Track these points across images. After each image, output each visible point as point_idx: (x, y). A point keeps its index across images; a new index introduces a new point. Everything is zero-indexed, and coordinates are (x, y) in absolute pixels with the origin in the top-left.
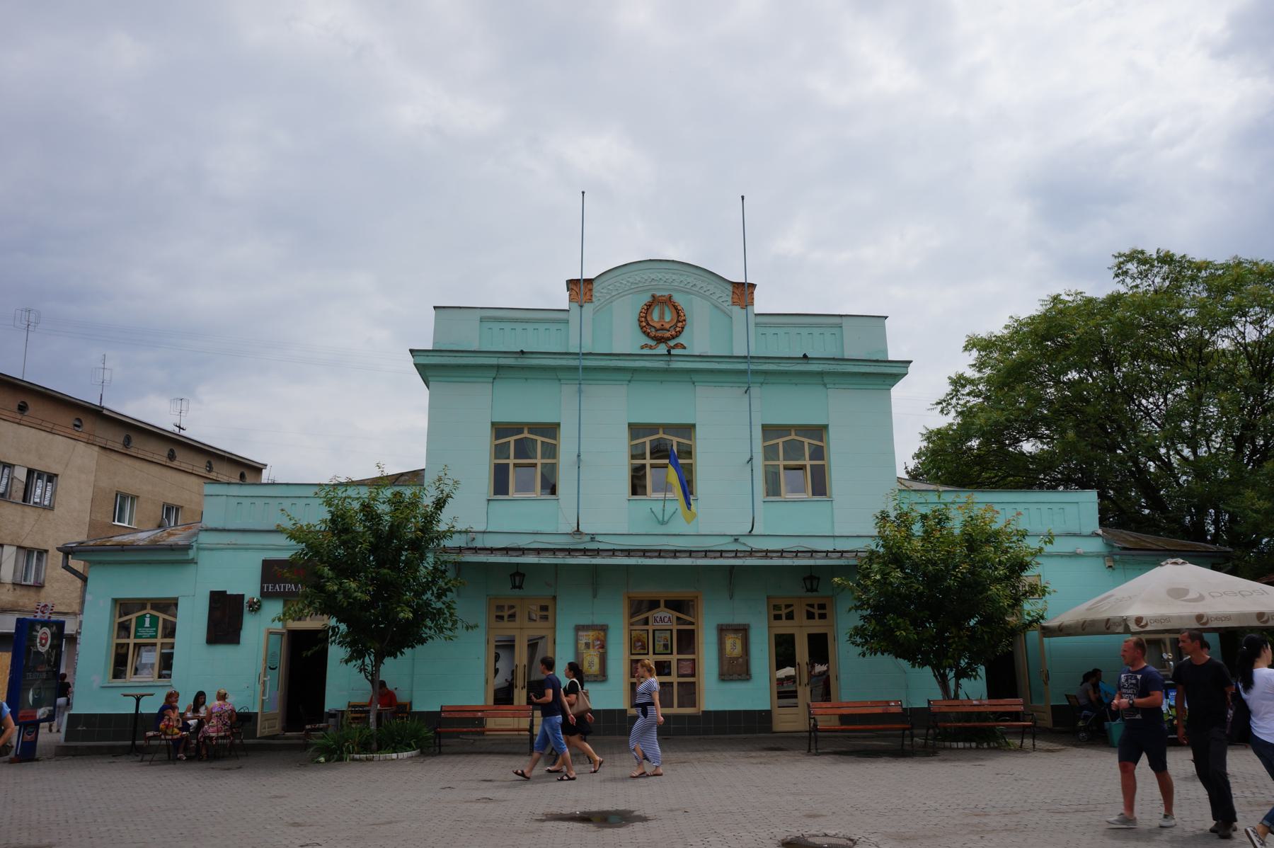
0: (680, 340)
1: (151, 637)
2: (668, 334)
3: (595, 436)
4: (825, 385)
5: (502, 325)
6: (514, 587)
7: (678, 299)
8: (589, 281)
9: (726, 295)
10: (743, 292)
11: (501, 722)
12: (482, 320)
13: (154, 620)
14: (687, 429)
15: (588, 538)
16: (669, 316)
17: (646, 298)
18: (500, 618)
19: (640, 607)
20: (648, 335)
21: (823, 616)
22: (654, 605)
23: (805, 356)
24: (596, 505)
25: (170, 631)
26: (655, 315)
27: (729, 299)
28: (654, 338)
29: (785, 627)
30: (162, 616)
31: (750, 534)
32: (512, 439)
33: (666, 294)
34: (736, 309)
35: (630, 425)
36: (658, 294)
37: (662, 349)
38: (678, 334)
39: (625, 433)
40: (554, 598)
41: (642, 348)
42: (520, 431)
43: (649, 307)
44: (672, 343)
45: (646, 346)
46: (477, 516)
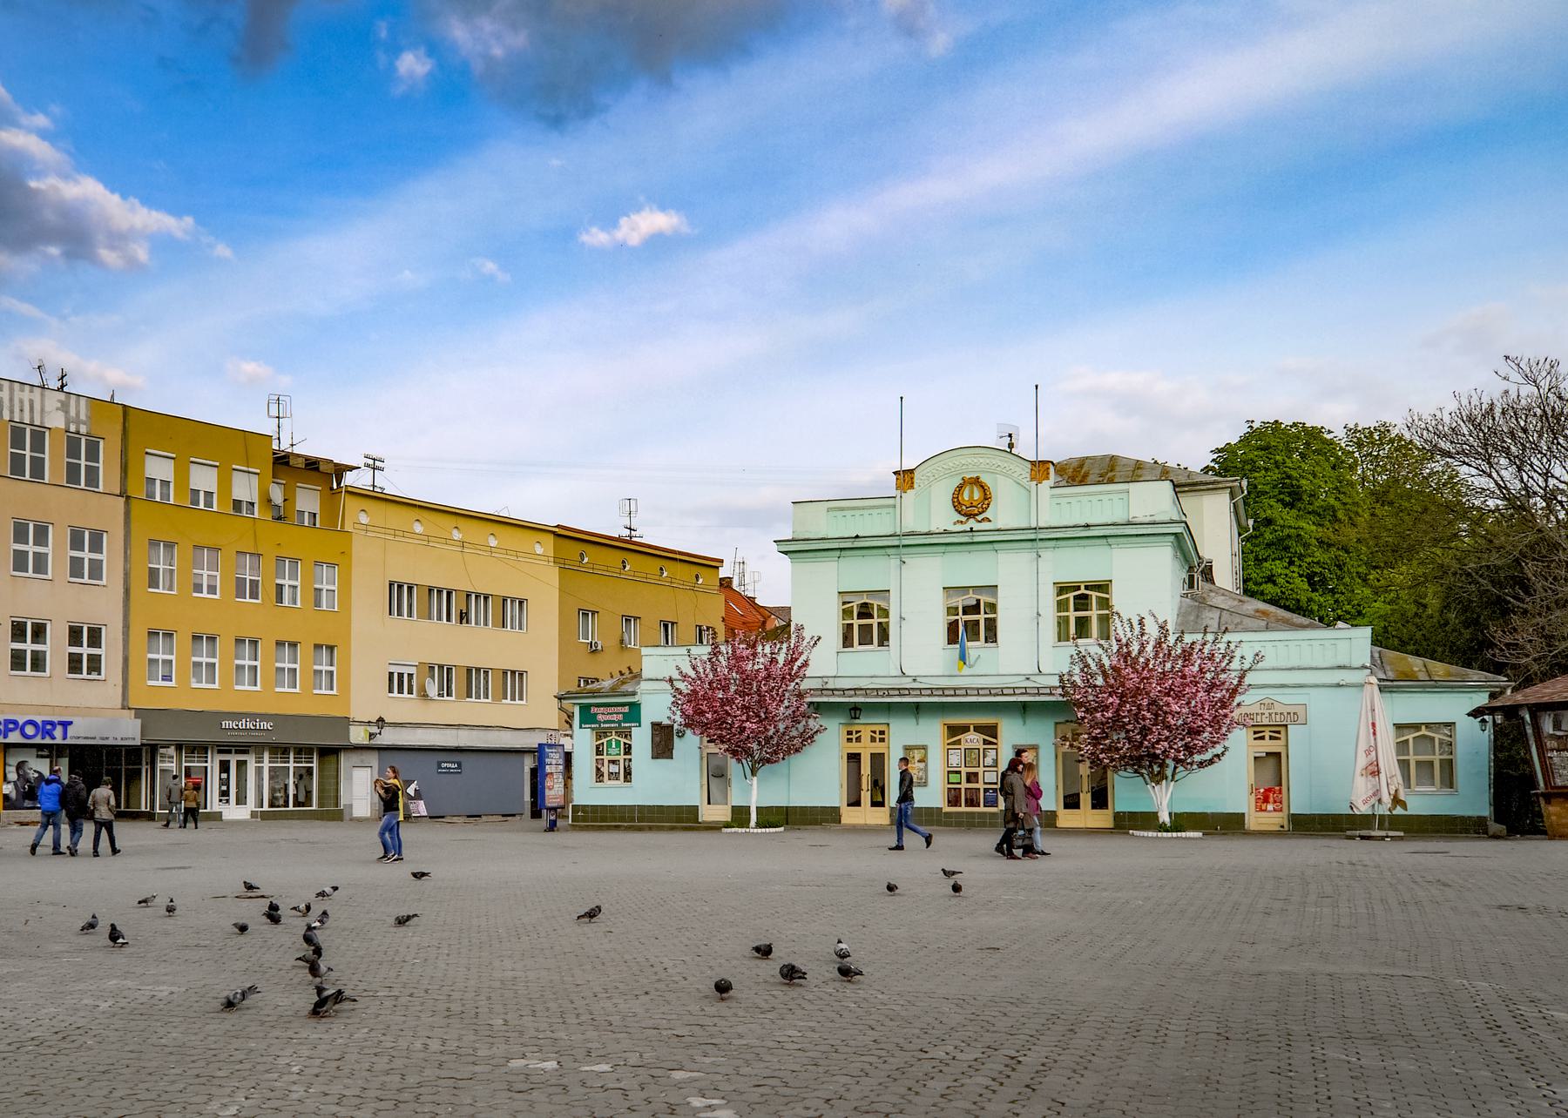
3: (919, 597)
8: (911, 471)
11: (850, 816)
13: (618, 742)
16: (977, 495)
17: (958, 481)
19: (954, 731)
22: (965, 729)
24: (919, 653)
25: (628, 750)
26: (966, 496)
30: (623, 740)
37: (972, 523)
43: (960, 487)
44: (979, 518)
46: (830, 663)
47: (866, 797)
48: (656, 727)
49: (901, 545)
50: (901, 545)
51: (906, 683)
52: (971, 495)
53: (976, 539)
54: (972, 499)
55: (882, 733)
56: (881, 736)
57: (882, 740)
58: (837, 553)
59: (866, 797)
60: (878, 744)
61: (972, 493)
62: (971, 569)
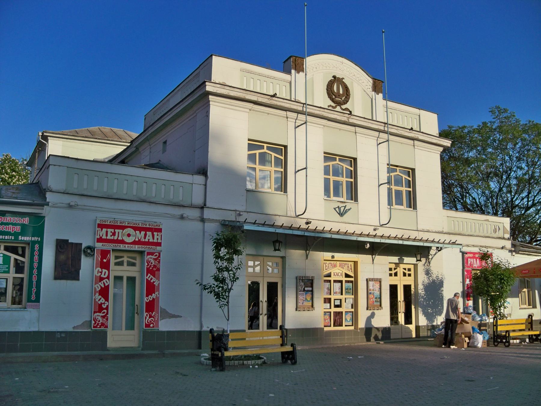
1: (5, 272)
6: (275, 250)
15: (305, 221)
18: (391, 275)
20: (333, 100)
23: (412, 129)
29: (394, 281)
30: (13, 256)
32: (257, 152)
38: (346, 102)
41: (329, 106)
42: (263, 147)
44: (344, 107)
45: (330, 106)
47: (263, 320)
48: (62, 245)
49: (304, 112)
50: (304, 112)
53: (351, 121)
54: (338, 92)
58: (251, 105)
59: (263, 320)
62: (344, 142)
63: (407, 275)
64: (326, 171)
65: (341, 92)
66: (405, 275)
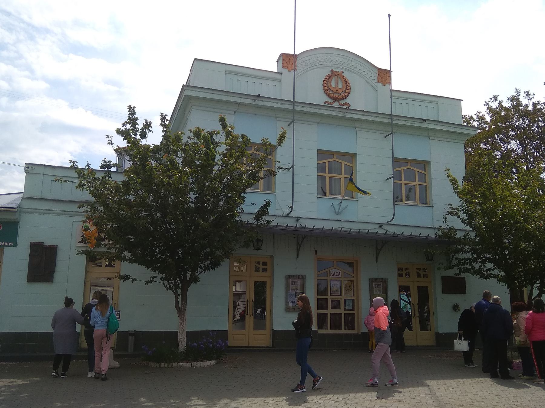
0: (348, 101)
2: (340, 97)
4: (429, 137)
5: (240, 78)
7: (346, 74)
8: (296, 55)
9: (375, 76)
10: (384, 76)
12: (227, 72)
14: (352, 156)
17: (327, 72)
20: (328, 95)
21: (425, 276)
26: (333, 84)
27: (376, 78)
28: (331, 98)
31: (387, 223)
33: (340, 71)
34: (380, 85)
35: (319, 151)
36: (335, 70)
39: (316, 155)
40: (272, 257)
41: (325, 103)
43: (329, 77)
44: (342, 102)
51: (291, 223)
52: (336, 85)
53: (349, 116)
55: (265, 264)
56: (264, 266)
57: (264, 270)
60: (261, 273)
61: (337, 84)
63: (422, 276)
64: (321, 168)
65: (340, 86)
66: (419, 275)
